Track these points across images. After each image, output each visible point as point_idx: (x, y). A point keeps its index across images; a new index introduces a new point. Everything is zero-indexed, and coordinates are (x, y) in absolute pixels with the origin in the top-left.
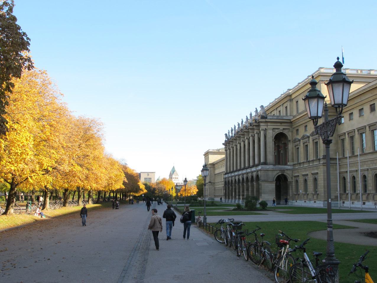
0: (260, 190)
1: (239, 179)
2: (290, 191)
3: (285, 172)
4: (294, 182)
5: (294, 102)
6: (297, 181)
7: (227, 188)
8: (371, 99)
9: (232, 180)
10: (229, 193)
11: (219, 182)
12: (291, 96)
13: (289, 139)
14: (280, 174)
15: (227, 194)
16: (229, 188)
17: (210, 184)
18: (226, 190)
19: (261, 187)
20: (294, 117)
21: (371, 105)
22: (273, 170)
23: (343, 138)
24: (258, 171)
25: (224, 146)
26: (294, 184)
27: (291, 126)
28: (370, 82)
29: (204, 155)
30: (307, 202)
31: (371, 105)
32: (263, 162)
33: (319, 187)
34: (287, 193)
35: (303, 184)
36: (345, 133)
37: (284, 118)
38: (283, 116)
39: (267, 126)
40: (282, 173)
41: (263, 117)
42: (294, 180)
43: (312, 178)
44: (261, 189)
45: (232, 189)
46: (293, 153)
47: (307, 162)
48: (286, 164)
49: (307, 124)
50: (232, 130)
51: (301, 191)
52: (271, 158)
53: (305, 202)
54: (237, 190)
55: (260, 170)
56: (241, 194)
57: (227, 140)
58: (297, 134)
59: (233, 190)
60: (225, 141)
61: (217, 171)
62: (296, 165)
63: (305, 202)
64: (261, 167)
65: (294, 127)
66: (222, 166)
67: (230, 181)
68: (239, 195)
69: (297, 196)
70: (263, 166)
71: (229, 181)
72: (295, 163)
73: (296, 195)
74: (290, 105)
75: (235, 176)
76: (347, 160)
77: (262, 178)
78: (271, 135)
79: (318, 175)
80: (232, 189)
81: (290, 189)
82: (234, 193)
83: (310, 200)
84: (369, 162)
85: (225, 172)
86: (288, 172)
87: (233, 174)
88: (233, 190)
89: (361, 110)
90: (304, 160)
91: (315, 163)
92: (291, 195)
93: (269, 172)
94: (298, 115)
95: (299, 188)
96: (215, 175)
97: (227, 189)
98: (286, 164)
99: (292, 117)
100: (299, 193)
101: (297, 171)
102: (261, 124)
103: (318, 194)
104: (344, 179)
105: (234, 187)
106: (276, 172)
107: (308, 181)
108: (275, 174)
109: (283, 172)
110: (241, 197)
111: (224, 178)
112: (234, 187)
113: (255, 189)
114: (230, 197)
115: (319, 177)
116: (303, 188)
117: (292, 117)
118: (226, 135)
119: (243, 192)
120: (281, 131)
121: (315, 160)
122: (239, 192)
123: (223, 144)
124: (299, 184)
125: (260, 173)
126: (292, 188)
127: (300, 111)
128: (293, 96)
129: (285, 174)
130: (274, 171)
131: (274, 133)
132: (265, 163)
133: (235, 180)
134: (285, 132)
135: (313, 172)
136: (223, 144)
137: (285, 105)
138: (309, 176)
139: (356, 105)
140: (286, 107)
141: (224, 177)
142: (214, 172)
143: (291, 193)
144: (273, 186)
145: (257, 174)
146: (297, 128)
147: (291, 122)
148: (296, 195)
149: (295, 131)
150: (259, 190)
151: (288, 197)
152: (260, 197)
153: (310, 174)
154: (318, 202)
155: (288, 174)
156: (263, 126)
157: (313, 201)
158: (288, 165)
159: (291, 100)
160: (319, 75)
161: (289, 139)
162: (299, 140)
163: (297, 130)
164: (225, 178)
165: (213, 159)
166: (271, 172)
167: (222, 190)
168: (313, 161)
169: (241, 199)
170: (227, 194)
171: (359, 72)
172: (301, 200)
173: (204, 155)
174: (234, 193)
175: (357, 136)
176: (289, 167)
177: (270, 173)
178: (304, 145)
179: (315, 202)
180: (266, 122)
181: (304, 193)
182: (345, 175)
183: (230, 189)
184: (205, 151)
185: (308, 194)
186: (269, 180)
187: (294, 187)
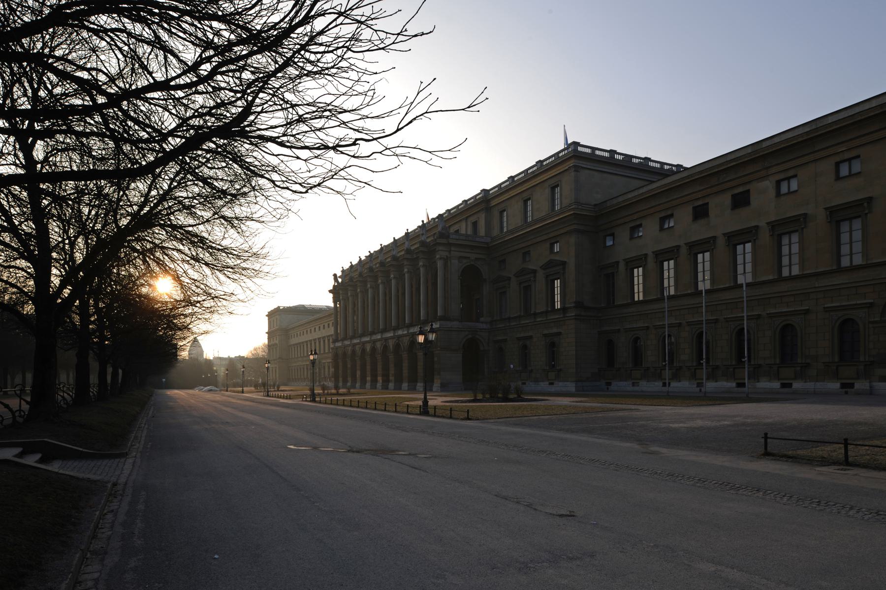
5: (496, 213)
14: (470, 336)
18: (336, 367)
21: (695, 208)
25: (331, 295)
36: (618, 263)
59: (358, 367)
61: (293, 341)
67: (350, 352)
82: (358, 373)
88: (358, 367)
99: (489, 240)
102: (441, 248)
118: (335, 275)
123: (330, 291)
128: (493, 203)
135: (546, 332)
136: (330, 291)
137: (473, 219)
140: (475, 224)
164: (337, 348)
174: (358, 373)
176: (484, 326)
180: (450, 245)
185: (531, 371)
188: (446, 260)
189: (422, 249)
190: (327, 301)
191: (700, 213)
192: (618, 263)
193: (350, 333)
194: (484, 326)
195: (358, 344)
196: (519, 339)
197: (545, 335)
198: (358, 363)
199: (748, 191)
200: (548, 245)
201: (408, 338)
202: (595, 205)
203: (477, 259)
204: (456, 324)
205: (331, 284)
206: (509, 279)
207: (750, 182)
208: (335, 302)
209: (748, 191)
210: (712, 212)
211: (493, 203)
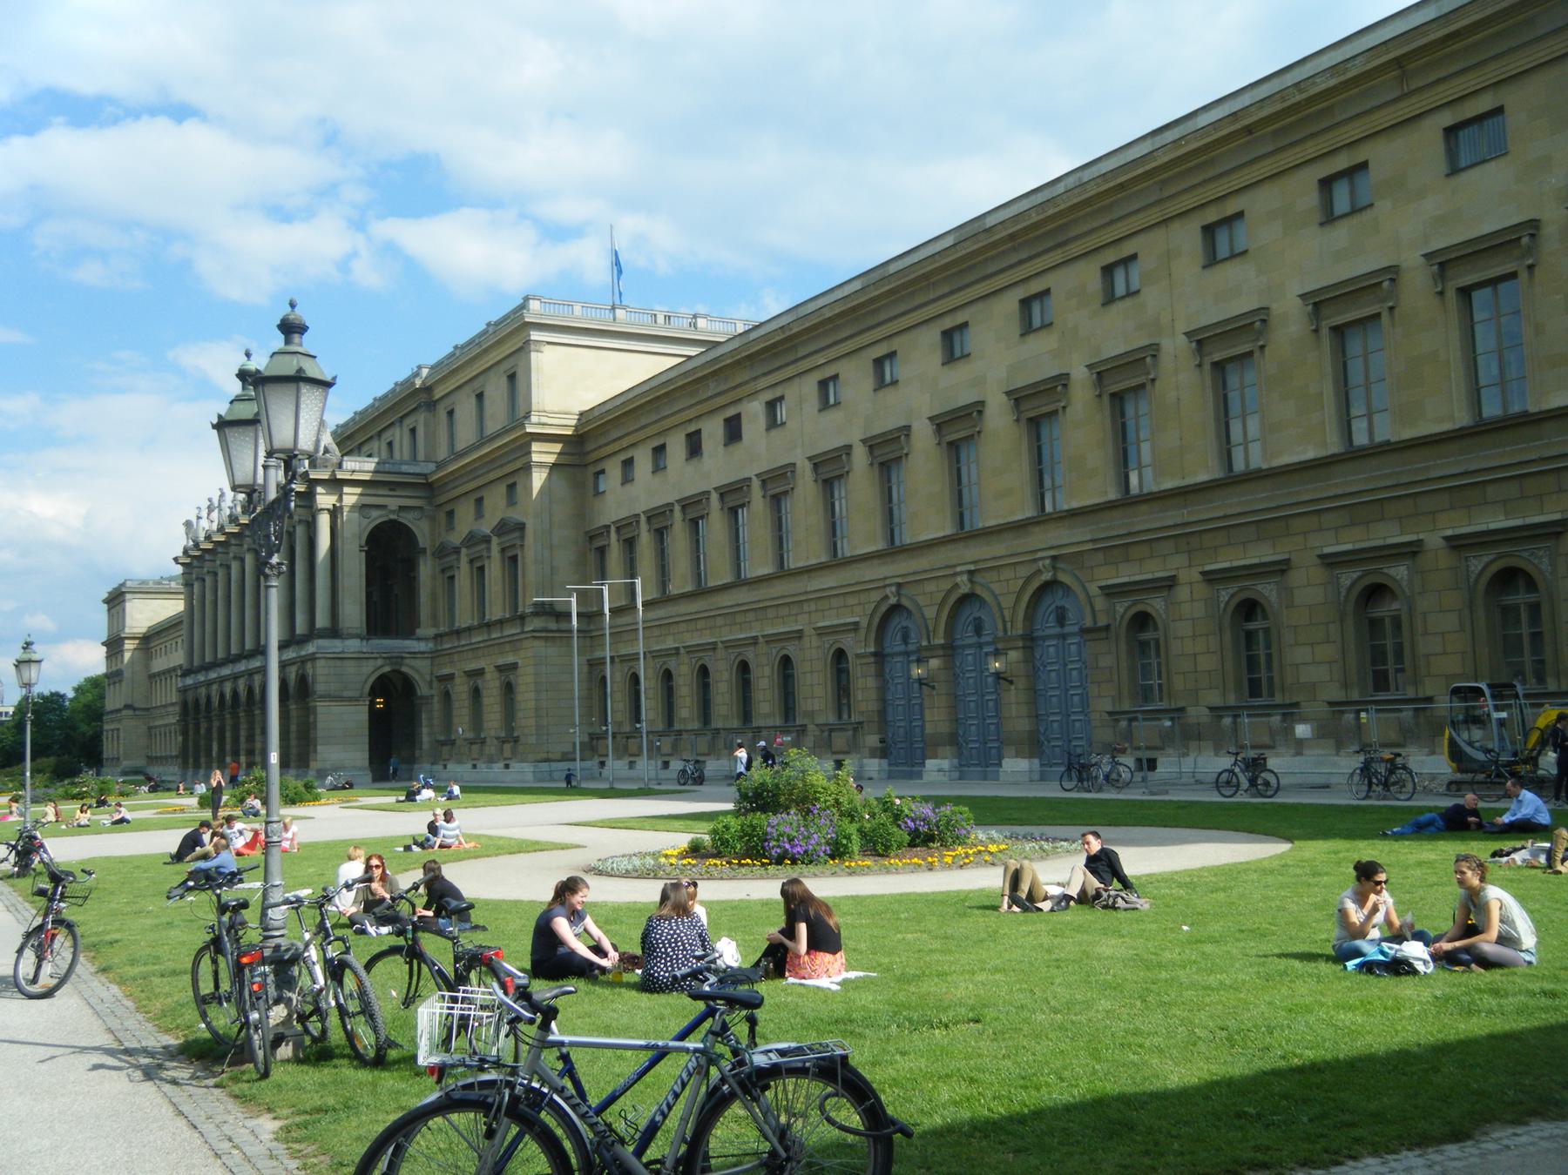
1: (235, 694)
2: (425, 730)
4: (436, 699)
6: (447, 696)
7: (191, 726)
8: (692, 413)
9: (209, 698)
14: (387, 669)
17: (130, 712)
18: (185, 733)
20: (440, 465)
21: (689, 436)
22: (360, 658)
26: (436, 705)
29: (107, 601)
30: (481, 765)
31: (689, 436)
33: (520, 715)
34: (412, 739)
35: (466, 703)
36: (607, 527)
37: (405, 468)
38: (402, 463)
42: (435, 691)
45: (209, 730)
47: (480, 626)
49: (484, 493)
50: (210, 509)
52: (353, 612)
53: (475, 766)
54: (228, 734)
56: (243, 746)
58: (450, 526)
59: (215, 735)
63: (475, 766)
65: (442, 499)
67: (203, 701)
68: (236, 753)
69: (446, 749)
70: (321, 642)
71: (197, 701)
73: (443, 743)
74: (426, 425)
75: (222, 680)
77: (320, 688)
79: (520, 671)
80: (209, 730)
81: (424, 722)
88: (215, 735)
89: (660, 451)
91: (510, 631)
92: (426, 746)
94: (455, 460)
95: (455, 720)
96: (152, 677)
97: (191, 733)
98: (409, 633)
99: (432, 467)
105: (216, 724)
106: (371, 662)
107: (484, 693)
108: (367, 672)
110: (243, 759)
111: (179, 690)
112: (216, 724)
114: (203, 760)
115: (520, 681)
116: (467, 719)
117: (432, 467)
118: (188, 524)
120: (393, 517)
121: (508, 620)
122: (236, 740)
124: (456, 705)
127: (460, 446)
128: (438, 394)
129: (404, 669)
132: (334, 632)
133: (222, 696)
134: (407, 519)
135: (501, 662)
136: (176, 559)
137: (409, 422)
138: (488, 676)
139: (641, 435)
140: (413, 431)
142: (147, 666)
143: (425, 739)
144: (358, 716)
146: (448, 508)
147: (429, 486)
148: (443, 743)
149: (442, 517)
151: (417, 753)
154: (516, 766)
155: (419, 672)
157: (501, 765)
158: (419, 639)
159: (431, 405)
162: (457, 551)
163: (451, 514)
166: (352, 663)
168: (501, 622)
172: (460, 762)
173: (107, 601)
175: (645, 539)
176: (422, 646)
177: (350, 668)
179: (507, 766)
181: (470, 735)
183: (202, 731)
185: (483, 742)
186: (346, 694)
187: (436, 714)
191: (694, 447)
194: (422, 646)
200: (502, 489)
203: (401, 508)
204: (353, 645)
205: (178, 543)
207: (740, 400)
210: (707, 446)
211: (438, 394)
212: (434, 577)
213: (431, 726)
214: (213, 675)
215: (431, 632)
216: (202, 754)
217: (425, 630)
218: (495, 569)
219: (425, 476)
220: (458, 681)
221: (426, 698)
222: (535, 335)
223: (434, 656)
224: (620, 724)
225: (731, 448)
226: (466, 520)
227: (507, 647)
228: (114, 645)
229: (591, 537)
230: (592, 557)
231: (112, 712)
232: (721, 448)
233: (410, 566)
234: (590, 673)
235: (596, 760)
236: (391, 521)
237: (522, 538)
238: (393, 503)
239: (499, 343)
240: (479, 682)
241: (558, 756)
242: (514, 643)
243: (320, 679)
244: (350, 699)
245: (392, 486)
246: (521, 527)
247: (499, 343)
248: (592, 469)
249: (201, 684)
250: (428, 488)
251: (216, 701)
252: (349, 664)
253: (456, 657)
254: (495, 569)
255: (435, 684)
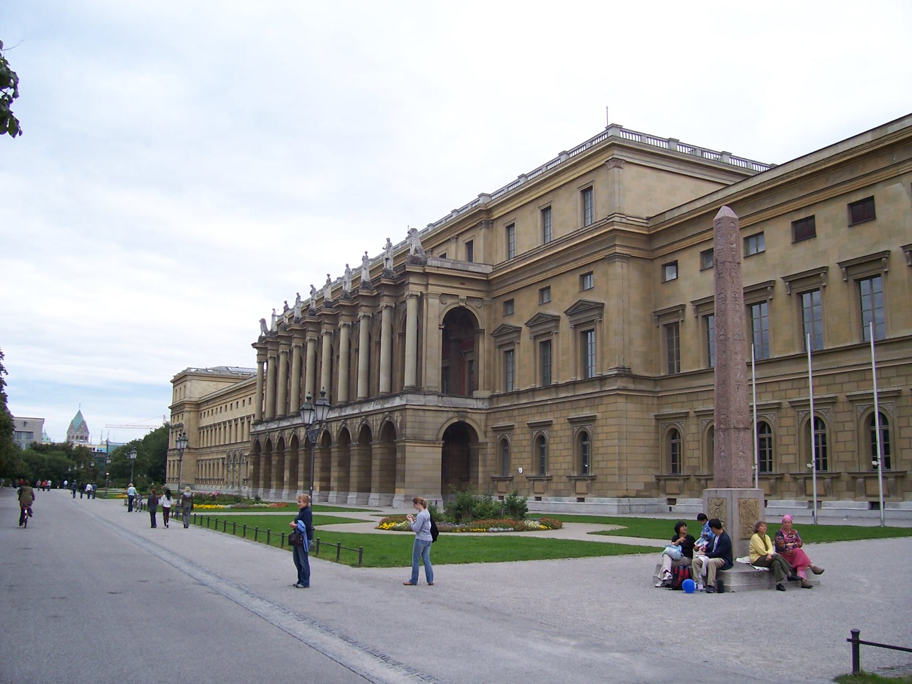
0: (399, 466)
2: (480, 469)
3: (469, 415)
4: (489, 445)
7: (262, 459)
9: (281, 440)
10: (268, 471)
11: (210, 447)
12: (489, 211)
13: (481, 327)
14: (456, 420)
15: (262, 475)
16: (269, 461)
18: (257, 464)
19: (404, 458)
20: (496, 268)
23: (672, 321)
24: (392, 411)
25: (256, 351)
27: (488, 292)
28: (728, 186)
32: (412, 387)
36: (683, 307)
39: (427, 285)
40: (461, 419)
41: (415, 261)
43: (569, 433)
44: (404, 463)
45: (281, 462)
46: (488, 366)
48: (470, 396)
49: (551, 283)
51: (521, 470)
52: (433, 375)
54: (301, 466)
55: (402, 409)
57: (264, 335)
60: (260, 337)
61: (206, 421)
62: (501, 399)
64: (405, 399)
65: (501, 292)
66: (229, 406)
68: (309, 481)
70: (410, 396)
72: (497, 392)
74: (485, 238)
76: (807, 362)
78: (436, 311)
82: (287, 474)
83: (558, 494)
84: (783, 386)
85: (257, 418)
86: (476, 417)
87: (285, 424)
90: (576, 374)
92: (480, 481)
93: (428, 413)
95: (514, 462)
97: (262, 463)
99: (489, 269)
100: (510, 475)
101: (504, 414)
102: (412, 280)
103: (593, 479)
104: (674, 434)
106: (445, 414)
109: (462, 417)
110: (317, 484)
112: (288, 459)
113: (376, 463)
114: (274, 483)
116: (529, 461)
118: (263, 322)
119: (326, 468)
122: (308, 470)
123: (254, 345)
124: (514, 450)
125: (401, 415)
126: (485, 461)
127: (520, 250)
128: (496, 214)
129: (468, 421)
130: (440, 413)
131: (444, 306)
132: (417, 389)
134: (472, 307)
135: (573, 415)
136: (254, 345)
137: (467, 237)
138: (556, 427)
140: (470, 245)
141: (252, 430)
142: (198, 422)
143: (480, 475)
144: (435, 454)
145: (387, 419)
146: (507, 298)
147: (488, 282)
150: (395, 465)
152: (397, 484)
153: (562, 420)
155: (476, 421)
156: (415, 287)
160: (613, 144)
161: (481, 327)
163: (511, 302)
164: (258, 433)
165: (197, 390)
167: (220, 465)
169: (318, 488)
170: (262, 475)
171: (699, 153)
174: (287, 474)
176: (480, 405)
177: (429, 418)
178: (535, 344)
180: (426, 275)
182: (680, 426)
183: (274, 463)
184: (179, 369)
185: (550, 479)
187: (489, 457)
188: (420, 299)
189: (384, 281)
190: (247, 360)
191: (804, 231)
192: (683, 307)
193: (280, 412)
194: (480, 405)
195: (288, 428)
196: (532, 426)
197: (572, 421)
198: (288, 459)
199: (872, 199)
200: (576, 278)
201: (359, 420)
202: (648, 219)
204: (432, 400)
205: (256, 334)
206: (518, 330)
208: (261, 363)
209: (872, 199)
210: (821, 228)
212: (489, 352)
213: (485, 466)
214: (285, 424)
215: (487, 394)
216: (273, 478)
217: (482, 393)
218: (564, 341)
219: (486, 275)
220: (517, 431)
221: (482, 444)
222: (617, 154)
223: (490, 413)
224: (695, 468)
225: (858, 228)
226: (527, 307)
227: (582, 403)
228: (176, 409)
229: (660, 315)
230: (661, 331)
231: (174, 450)
232: (844, 230)
233: (470, 345)
234: (657, 426)
235: (664, 498)
236: (461, 308)
237: (601, 316)
238: (463, 294)
239: (575, 165)
240: (545, 432)
241: (633, 493)
242: (590, 400)
243: (409, 425)
244: (428, 442)
245: (463, 280)
246: (600, 307)
247: (575, 165)
248: (659, 263)
249: (273, 430)
250: (487, 282)
251: (288, 442)
252: (427, 415)
253: (516, 413)
254: (564, 341)
255: (490, 434)
